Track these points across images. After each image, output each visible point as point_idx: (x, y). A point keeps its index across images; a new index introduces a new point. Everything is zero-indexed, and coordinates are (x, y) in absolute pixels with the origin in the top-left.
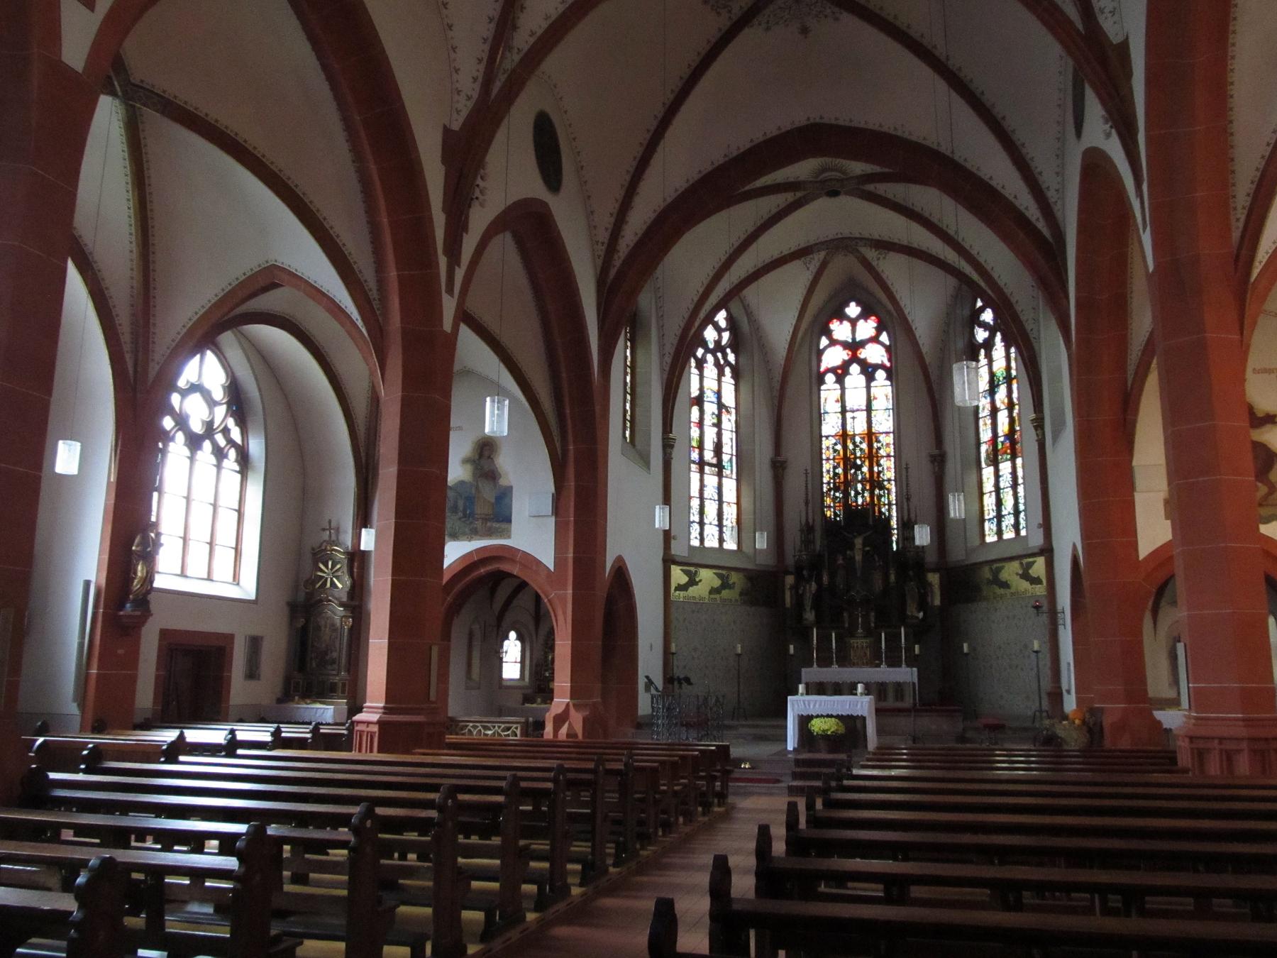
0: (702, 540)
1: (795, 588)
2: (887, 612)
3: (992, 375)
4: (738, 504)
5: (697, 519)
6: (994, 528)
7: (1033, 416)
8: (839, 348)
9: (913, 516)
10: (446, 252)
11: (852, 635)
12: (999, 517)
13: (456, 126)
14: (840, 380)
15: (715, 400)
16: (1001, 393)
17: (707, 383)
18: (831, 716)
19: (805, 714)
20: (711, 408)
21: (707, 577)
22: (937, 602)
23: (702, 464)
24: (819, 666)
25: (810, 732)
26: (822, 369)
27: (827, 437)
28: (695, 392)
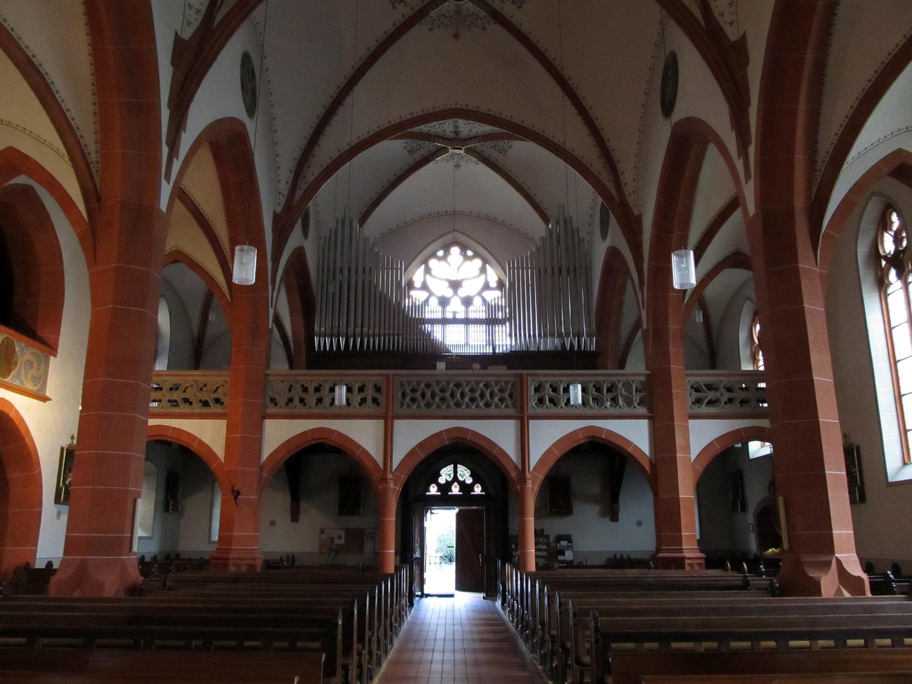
10: (168, 144)
13: (187, 34)
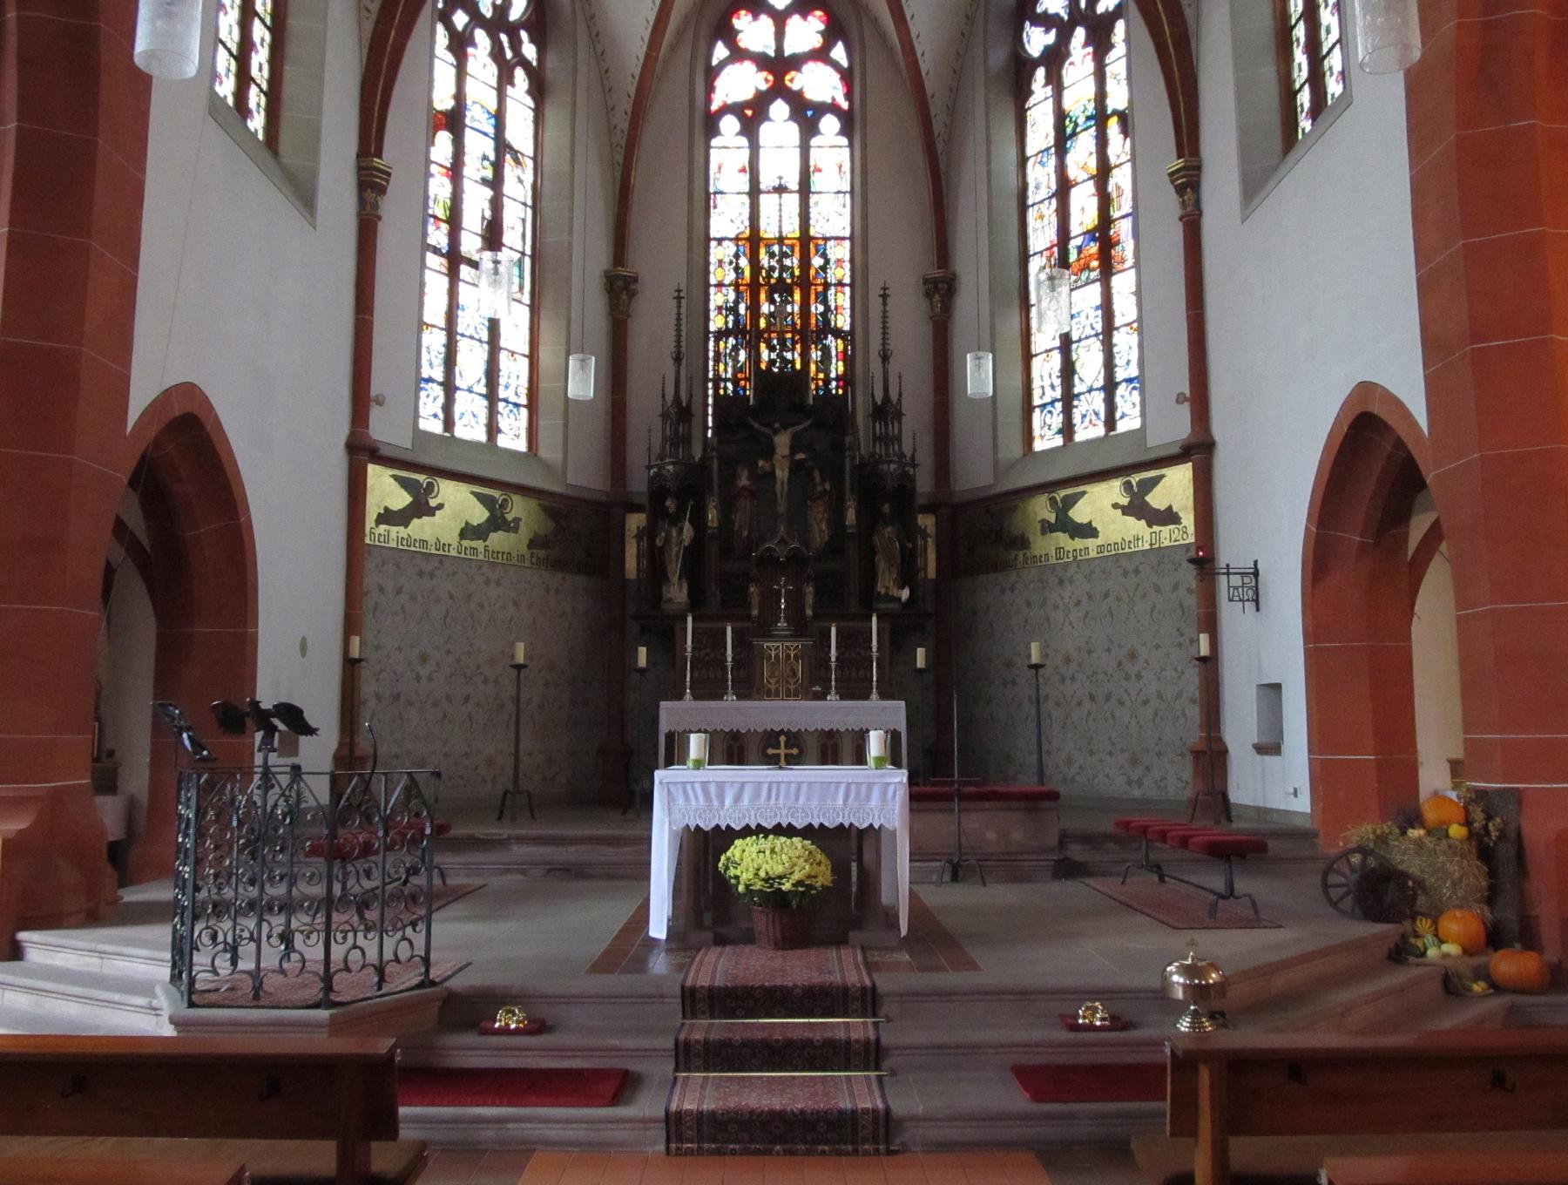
0: (449, 423)
1: (648, 533)
2: (839, 587)
3: (1061, 116)
4: (533, 357)
5: (439, 374)
6: (1057, 421)
7: (1180, 163)
8: (748, 67)
9: (894, 395)
11: (766, 630)
12: (1068, 399)
14: (750, 129)
15: (491, 131)
16: (1082, 154)
17: (473, 90)
18: (788, 831)
19: (707, 826)
20: (478, 146)
21: (458, 503)
22: (932, 572)
23: (454, 258)
24: (696, 697)
25: (724, 885)
26: (714, 107)
27: (720, 241)
28: (443, 100)
